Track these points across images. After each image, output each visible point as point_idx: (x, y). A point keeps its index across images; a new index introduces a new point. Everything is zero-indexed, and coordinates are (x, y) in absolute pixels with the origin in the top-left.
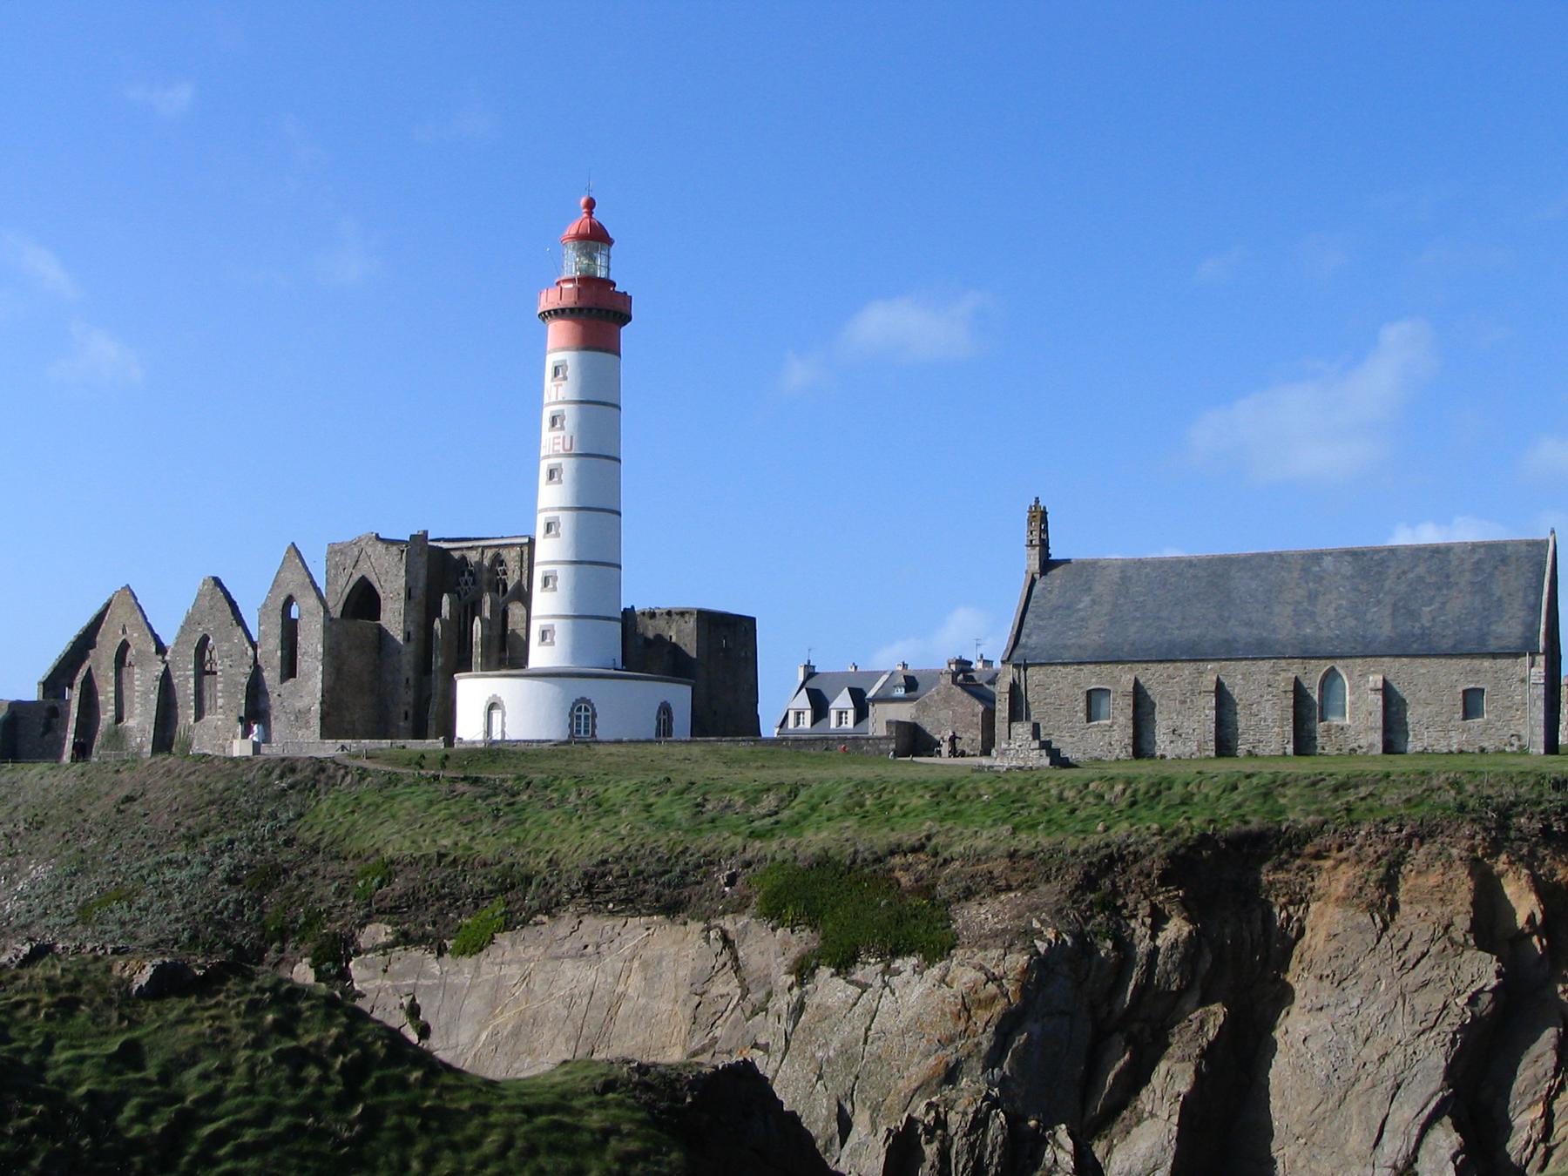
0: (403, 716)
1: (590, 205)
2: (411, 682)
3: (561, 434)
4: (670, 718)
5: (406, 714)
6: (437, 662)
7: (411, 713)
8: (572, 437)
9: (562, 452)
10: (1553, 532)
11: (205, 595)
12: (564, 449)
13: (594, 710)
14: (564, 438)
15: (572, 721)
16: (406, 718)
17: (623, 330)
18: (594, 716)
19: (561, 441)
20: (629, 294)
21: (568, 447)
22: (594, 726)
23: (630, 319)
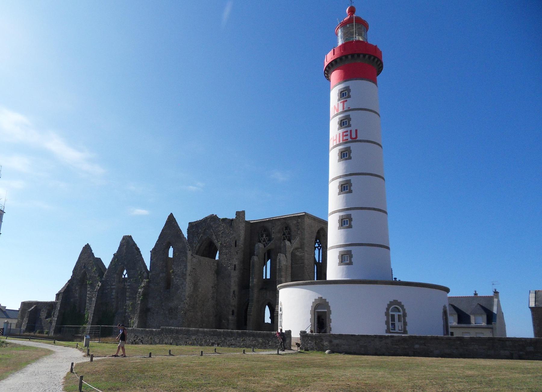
0: (231, 313)
2: (236, 293)
3: (349, 129)
5: (233, 311)
6: (253, 281)
7: (236, 311)
8: (356, 131)
9: (350, 140)
11: (124, 245)
12: (351, 138)
13: (404, 310)
14: (351, 131)
15: (388, 318)
16: (233, 314)
18: (405, 315)
19: (349, 133)
21: (354, 136)
22: (405, 324)
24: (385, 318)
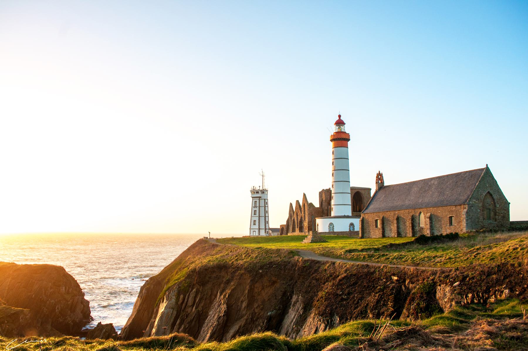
1: (340, 116)
4: (354, 226)
10: (487, 165)
13: (333, 225)
17: (349, 142)
18: (334, 226)
20: (350, 134)
22: (334, 229)
23: (350, 140)
24: (328, 228)
